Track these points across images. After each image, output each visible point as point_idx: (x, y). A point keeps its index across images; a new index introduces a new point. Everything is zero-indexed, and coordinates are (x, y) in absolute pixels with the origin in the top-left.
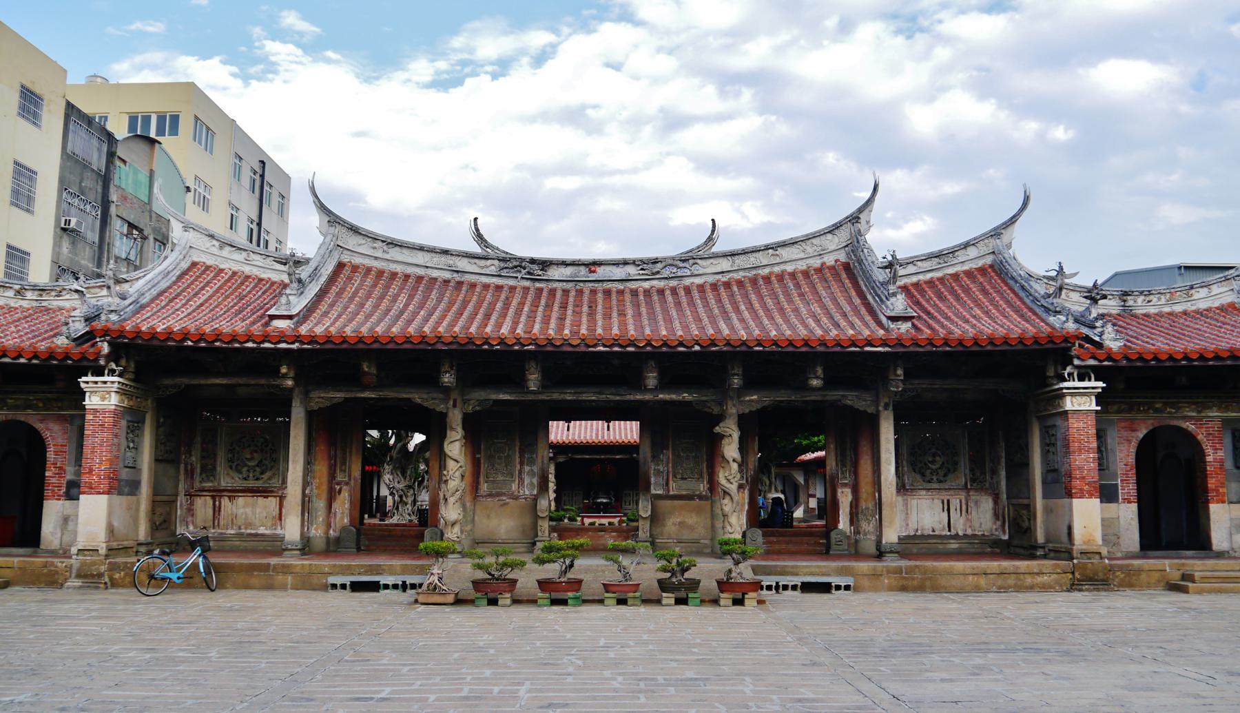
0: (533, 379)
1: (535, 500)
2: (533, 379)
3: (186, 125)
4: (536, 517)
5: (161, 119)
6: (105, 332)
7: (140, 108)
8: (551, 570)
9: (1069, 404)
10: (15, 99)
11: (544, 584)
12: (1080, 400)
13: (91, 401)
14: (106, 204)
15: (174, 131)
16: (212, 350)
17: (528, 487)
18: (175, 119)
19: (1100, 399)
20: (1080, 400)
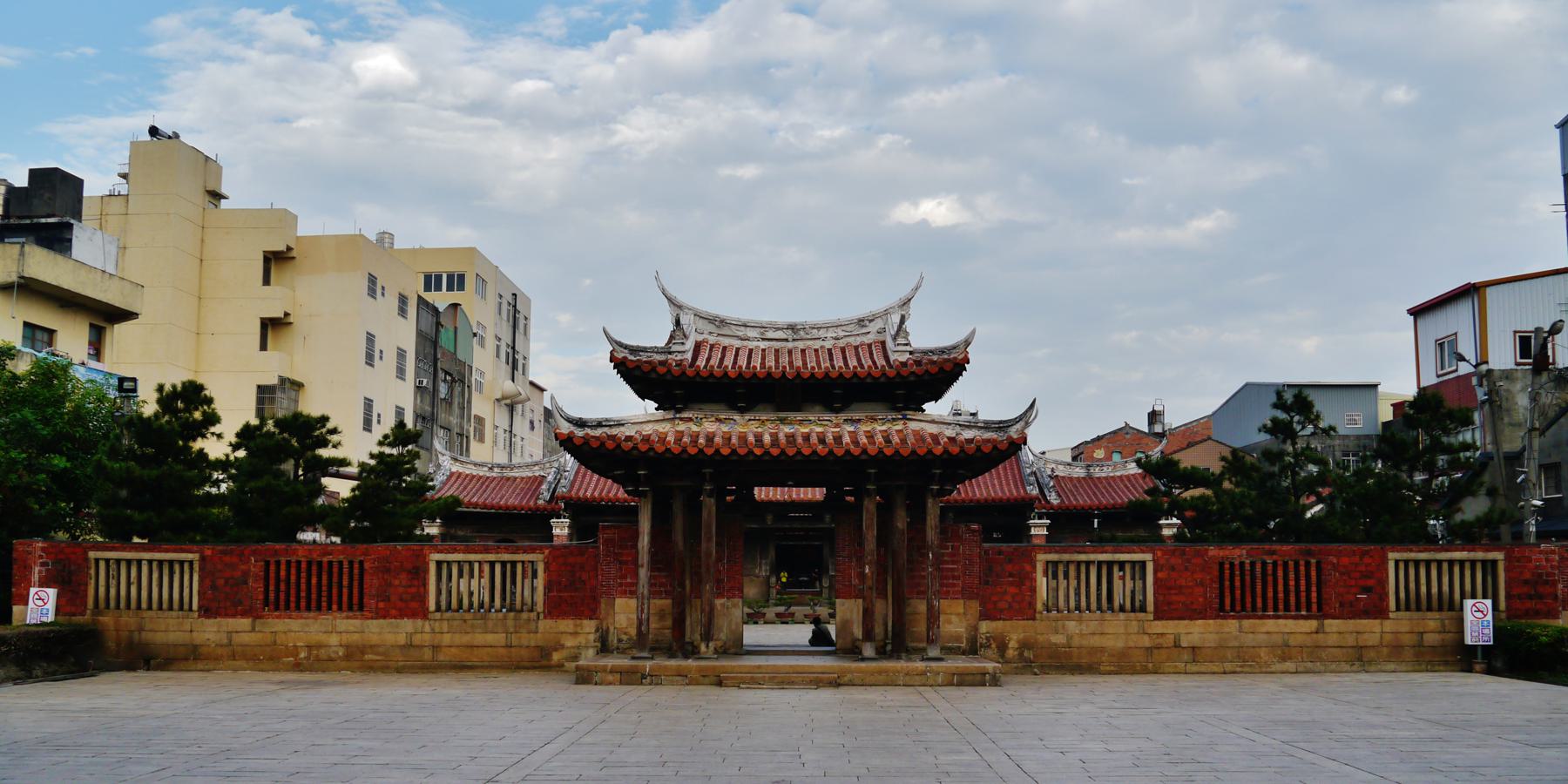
0: (769, 518)
1: (768, 578)
2: (769, 518)
3: (470, 282)
4: (769, 587)
5: (450, 277)
6: (563, 498)
7: (434, 268)
8: (781, 609)
9: (1033, 532)
10: (396, 303)
11: (778, 615)
12: (1039, 528)
13: (556, 531)
14: (435, 360)
15: (461, 287)
16: (614, 506)
17: (764, 571)
18: (462, 277)
19: (1049, 528)
20: (1039, 528)
